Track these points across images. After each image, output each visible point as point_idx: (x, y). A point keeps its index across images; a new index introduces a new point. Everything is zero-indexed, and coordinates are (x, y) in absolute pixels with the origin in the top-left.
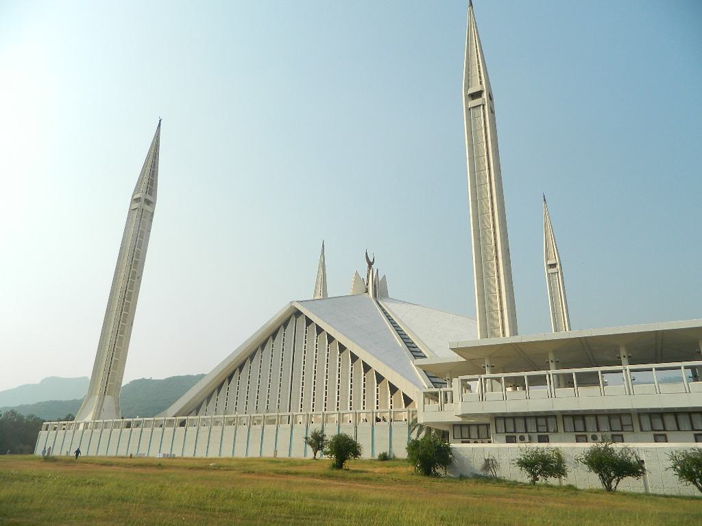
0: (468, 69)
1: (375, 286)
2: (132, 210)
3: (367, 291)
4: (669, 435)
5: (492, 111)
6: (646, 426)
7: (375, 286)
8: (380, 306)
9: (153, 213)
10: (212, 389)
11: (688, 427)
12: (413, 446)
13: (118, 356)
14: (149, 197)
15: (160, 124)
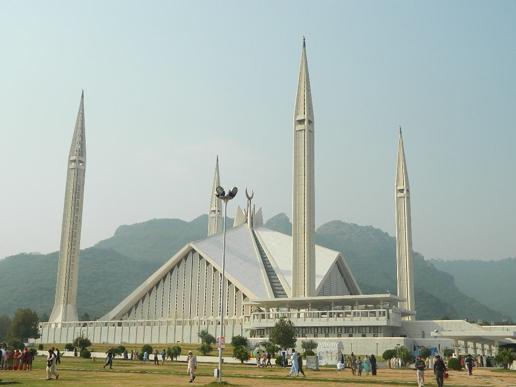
0: (298, 99)
1: (252, 218)
2: (69, 169)
3: (247, 222)
4: (319, 335)
5: (311, 132)
6: (313, 332)
7: (252, 218)
8: (255, 235)
9: (85, 170)
10: (139, 299)
11: (323, 332)
12: (234, 338)
13: (72, 278)
14: (81, 159)
15: (83, 95)
